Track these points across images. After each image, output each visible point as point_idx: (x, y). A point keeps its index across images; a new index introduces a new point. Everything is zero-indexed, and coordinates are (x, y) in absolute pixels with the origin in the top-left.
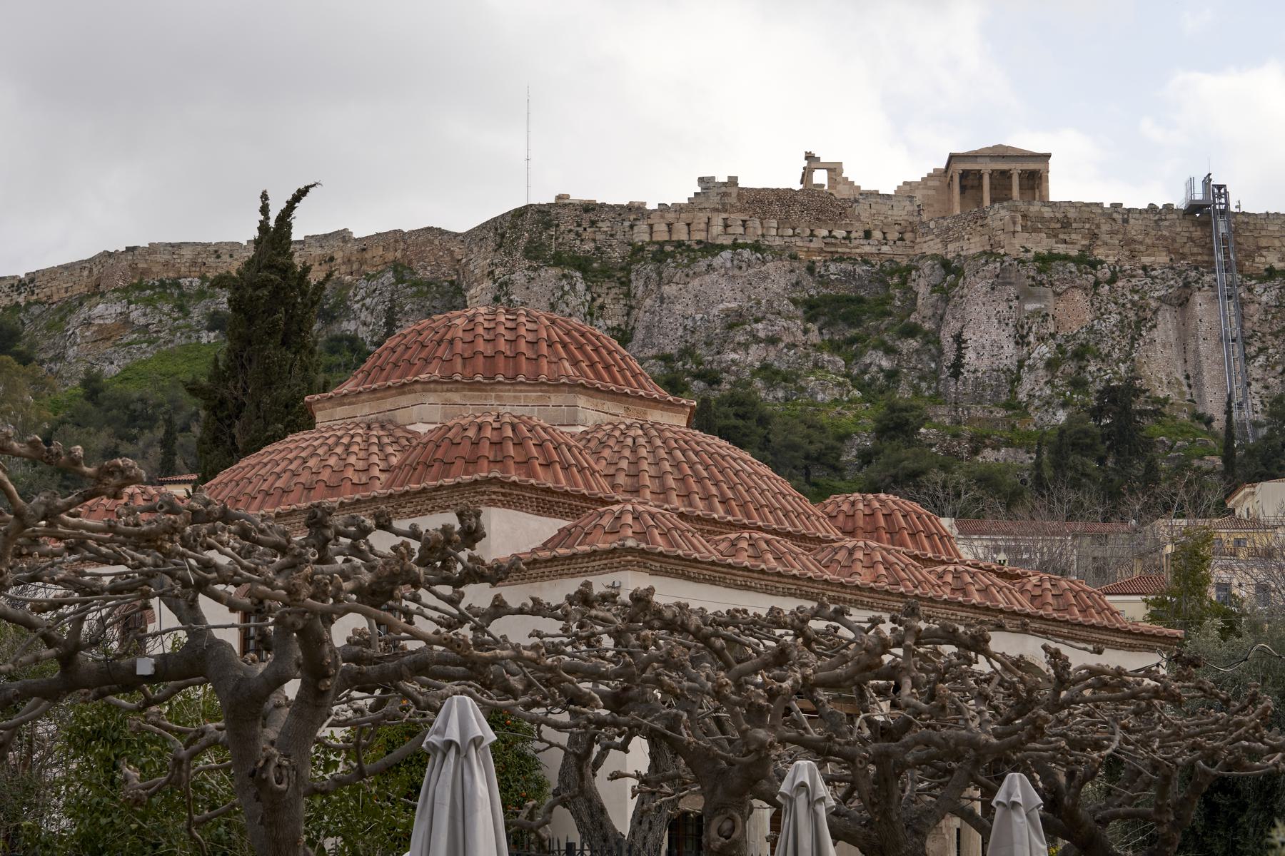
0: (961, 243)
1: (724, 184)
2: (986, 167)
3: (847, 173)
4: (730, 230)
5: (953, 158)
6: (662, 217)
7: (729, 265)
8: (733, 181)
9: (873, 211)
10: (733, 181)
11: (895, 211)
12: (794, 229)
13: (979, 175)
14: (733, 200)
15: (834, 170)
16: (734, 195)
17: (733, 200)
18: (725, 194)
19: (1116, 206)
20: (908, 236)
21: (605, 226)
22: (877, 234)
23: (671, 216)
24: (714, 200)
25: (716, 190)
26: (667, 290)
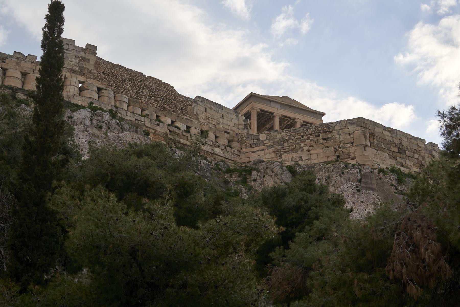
0: (300, 154)
1: (82, 49)
4: (85, 93)
6: (18, 64)
7: (88, 123)
8: (91, 49)
9: (209, 115)
10: (91, 49)
11: (225, 121)
12: (143, 110)
14: (90, 66)
16: (92, 62)
18: (83, 59)
20: (235, 145)
23: (27, 66)
25: (75, 53)
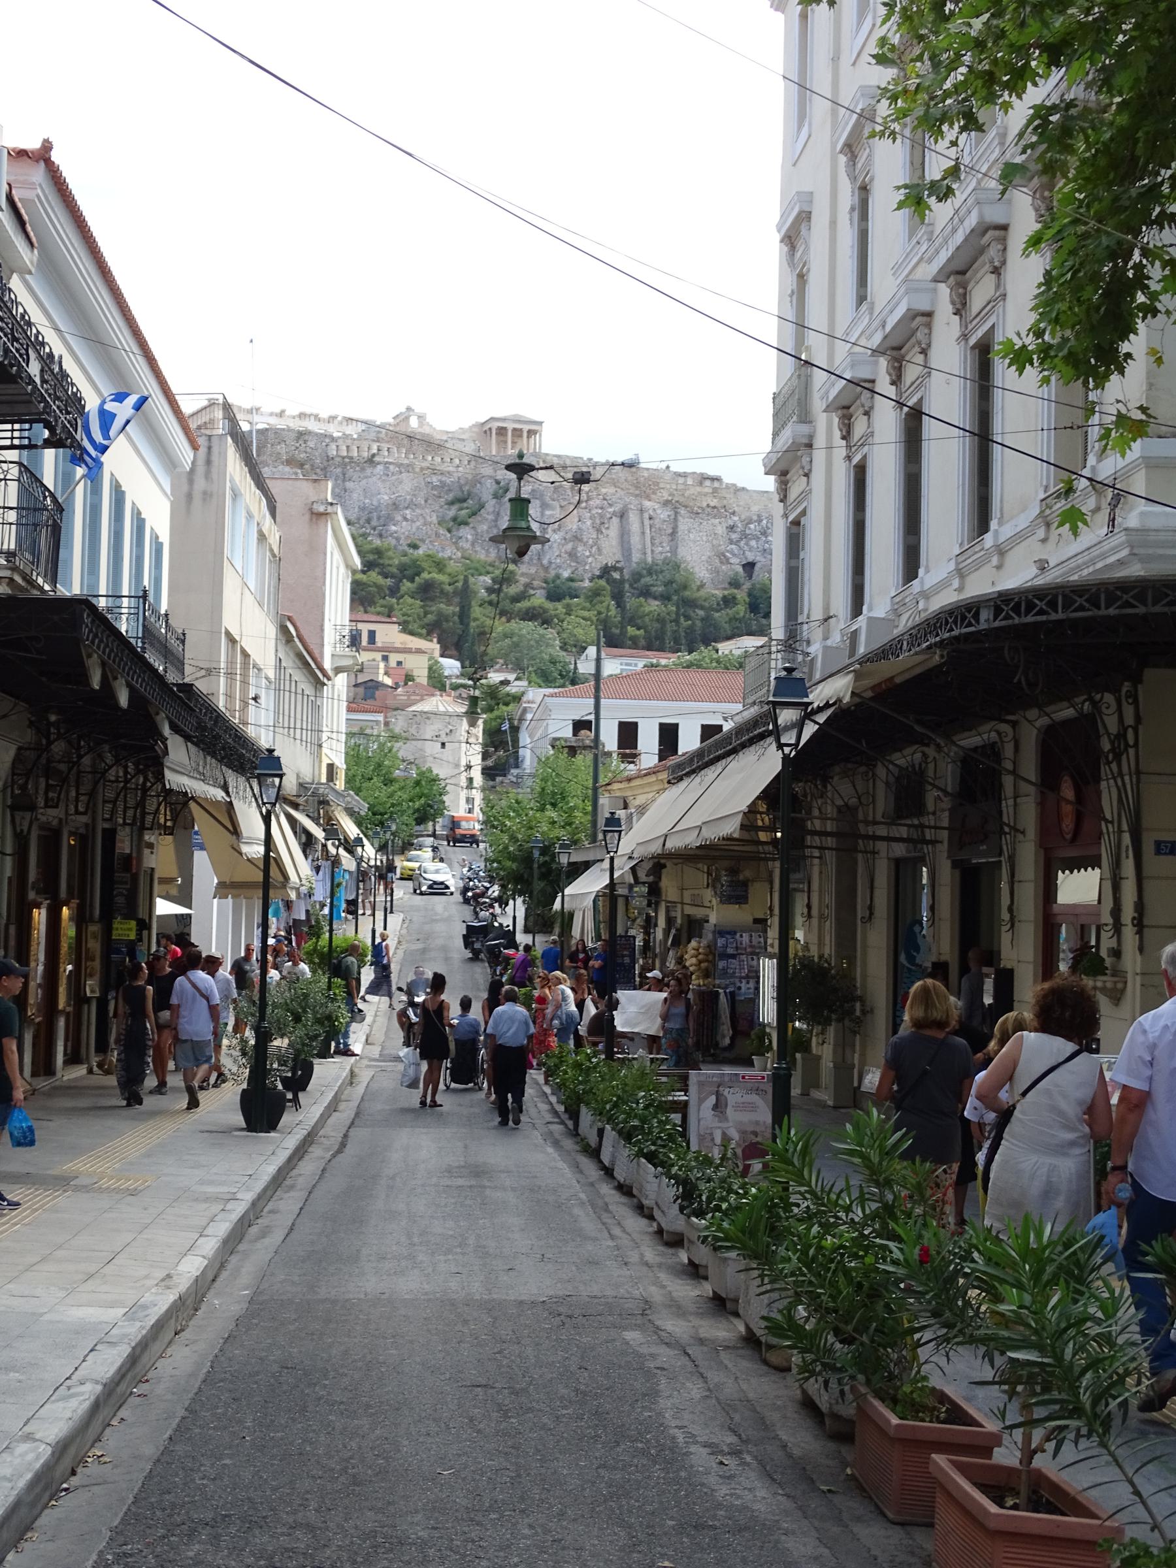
2: (510, 426)
3: (429, 419)
5: (492, 418)
13: (505, 429)
15: (421, 418)
17: (383, 435)
18: (379, 432)
19: (590, 460)
21: (311, 444)
22: (457, 461)
23: (349, 442)
24: (373, 435)
26: (349, 485)
